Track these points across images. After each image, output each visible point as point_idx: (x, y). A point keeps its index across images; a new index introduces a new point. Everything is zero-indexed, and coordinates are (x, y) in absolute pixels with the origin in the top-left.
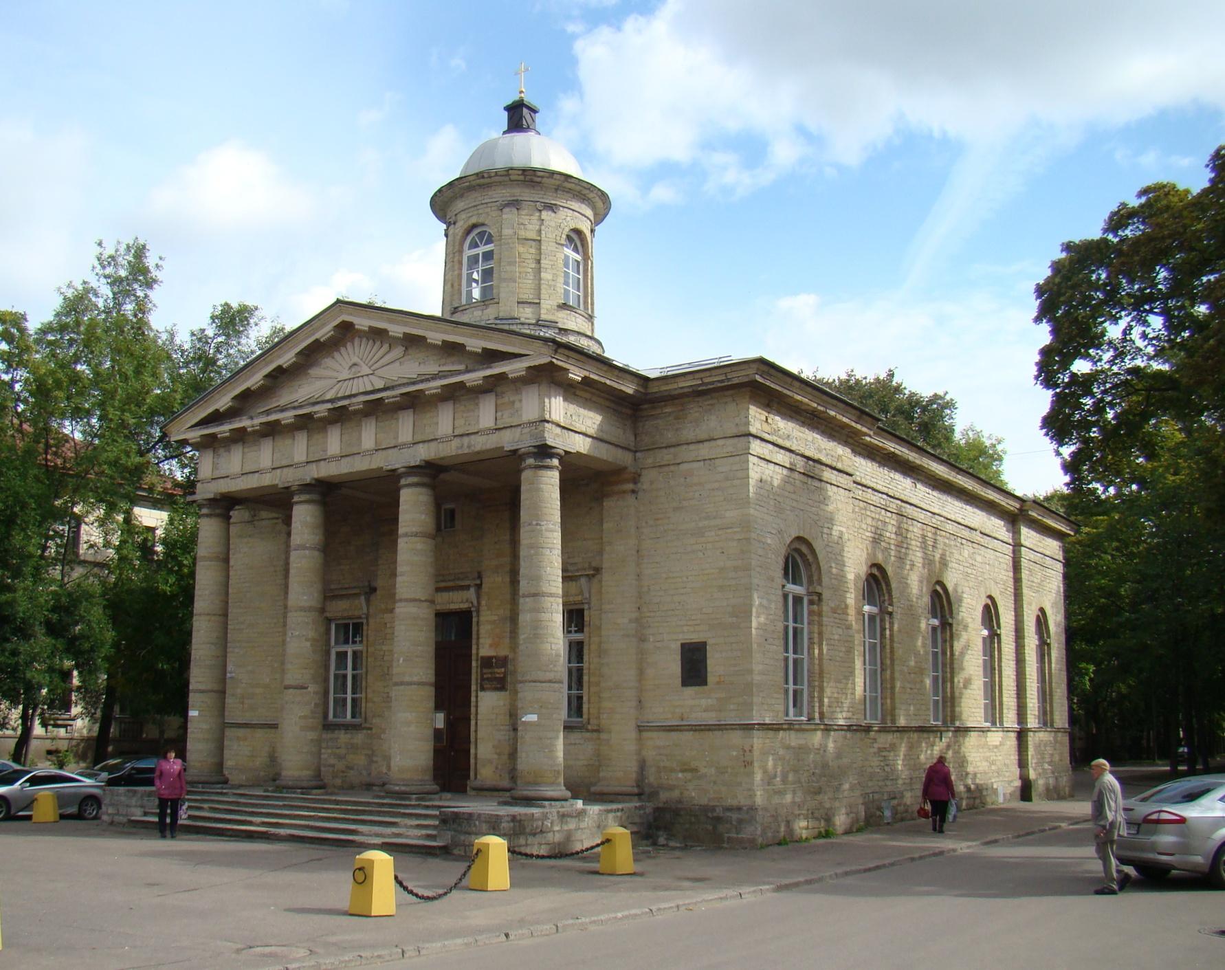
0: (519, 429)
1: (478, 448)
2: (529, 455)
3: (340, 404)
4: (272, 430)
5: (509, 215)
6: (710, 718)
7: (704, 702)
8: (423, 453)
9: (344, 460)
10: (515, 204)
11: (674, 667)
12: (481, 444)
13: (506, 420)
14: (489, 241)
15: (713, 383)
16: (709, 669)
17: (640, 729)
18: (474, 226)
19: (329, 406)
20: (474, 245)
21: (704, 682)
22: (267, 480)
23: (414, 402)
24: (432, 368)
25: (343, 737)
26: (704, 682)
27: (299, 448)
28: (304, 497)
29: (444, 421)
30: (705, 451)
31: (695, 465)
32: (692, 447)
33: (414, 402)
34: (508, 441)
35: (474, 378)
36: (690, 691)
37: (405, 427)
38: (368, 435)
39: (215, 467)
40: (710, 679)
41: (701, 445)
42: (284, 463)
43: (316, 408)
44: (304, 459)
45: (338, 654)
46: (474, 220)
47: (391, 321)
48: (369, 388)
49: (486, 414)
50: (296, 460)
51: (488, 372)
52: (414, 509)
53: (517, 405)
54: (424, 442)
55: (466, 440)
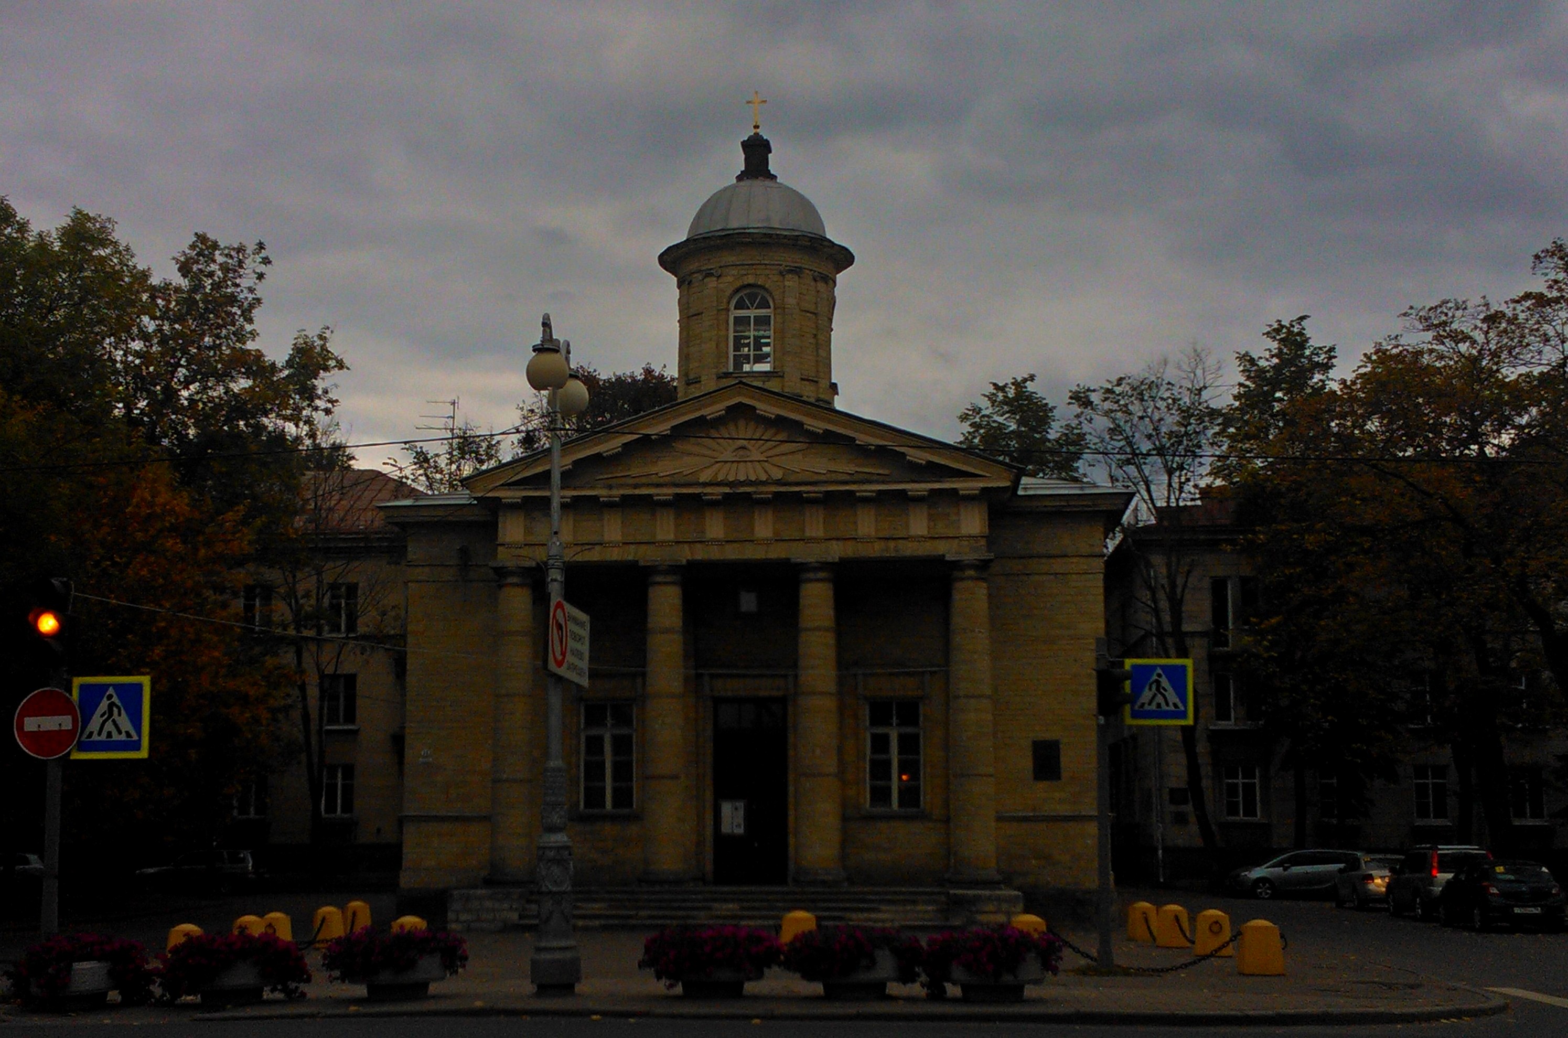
0: (956, 541)
1: (908, 553)
2: (971, 566)
3: (742, 490)
4: (629, 504)
5: (791, 282)
6: (1064, 810)
7: (1057, 795)
8: (836, 551)
9: (728, 547)
10: (797, 271)
11: (1026, 763)
12: (909, 549)
13: (941, 529)
14: (764, 305)
15: (1075, 506)
16: (1062, 765)
17: (1000, 819)
18: (749, 286)
19: (727, 490)
20: (739, 306)
21: (1059, 778)
22: (614, 555)
23: (837, 501)
24: (845, 466)
25: (609, 829)
26: (1059, 778)
27: (665, 528)
28: (669, 579)
29: (866, 524)
30: (1058, 566)
31: (1045, 578)
32: (1044, 560)
33: (837, 501)
34: (948, 550)
35: (922, 488)
36: (1042, 785)
37: (815, 524)
38: (764, 526)
39: (528, 531)
40: (1065, 774)
41: (1052, 560)
42: (639, 538)
43: (708, 490)
44: (671, 537)
45: (589, 739)
46: (750, 280)
47: (808, 415)
48: (764, 477)
49: (918, 523)
50: (659, 537)
51: (937, 486)
52: (817, 601)
53: (954, 518)
54: (838, 539)
55: (892, 544)
